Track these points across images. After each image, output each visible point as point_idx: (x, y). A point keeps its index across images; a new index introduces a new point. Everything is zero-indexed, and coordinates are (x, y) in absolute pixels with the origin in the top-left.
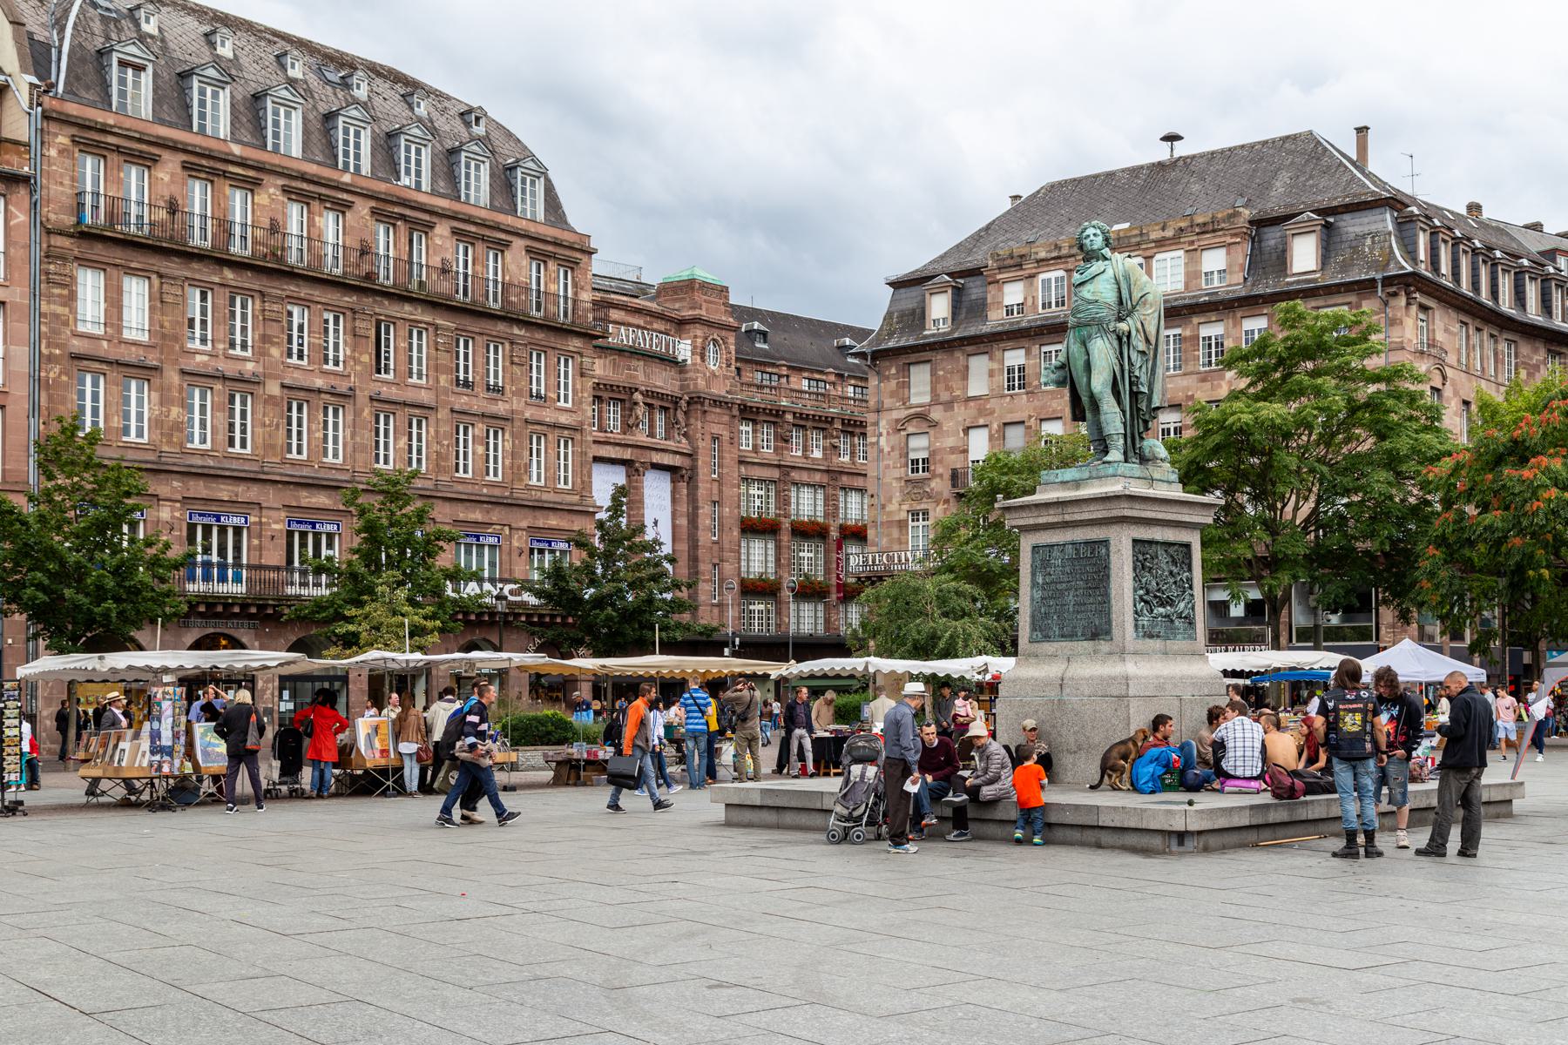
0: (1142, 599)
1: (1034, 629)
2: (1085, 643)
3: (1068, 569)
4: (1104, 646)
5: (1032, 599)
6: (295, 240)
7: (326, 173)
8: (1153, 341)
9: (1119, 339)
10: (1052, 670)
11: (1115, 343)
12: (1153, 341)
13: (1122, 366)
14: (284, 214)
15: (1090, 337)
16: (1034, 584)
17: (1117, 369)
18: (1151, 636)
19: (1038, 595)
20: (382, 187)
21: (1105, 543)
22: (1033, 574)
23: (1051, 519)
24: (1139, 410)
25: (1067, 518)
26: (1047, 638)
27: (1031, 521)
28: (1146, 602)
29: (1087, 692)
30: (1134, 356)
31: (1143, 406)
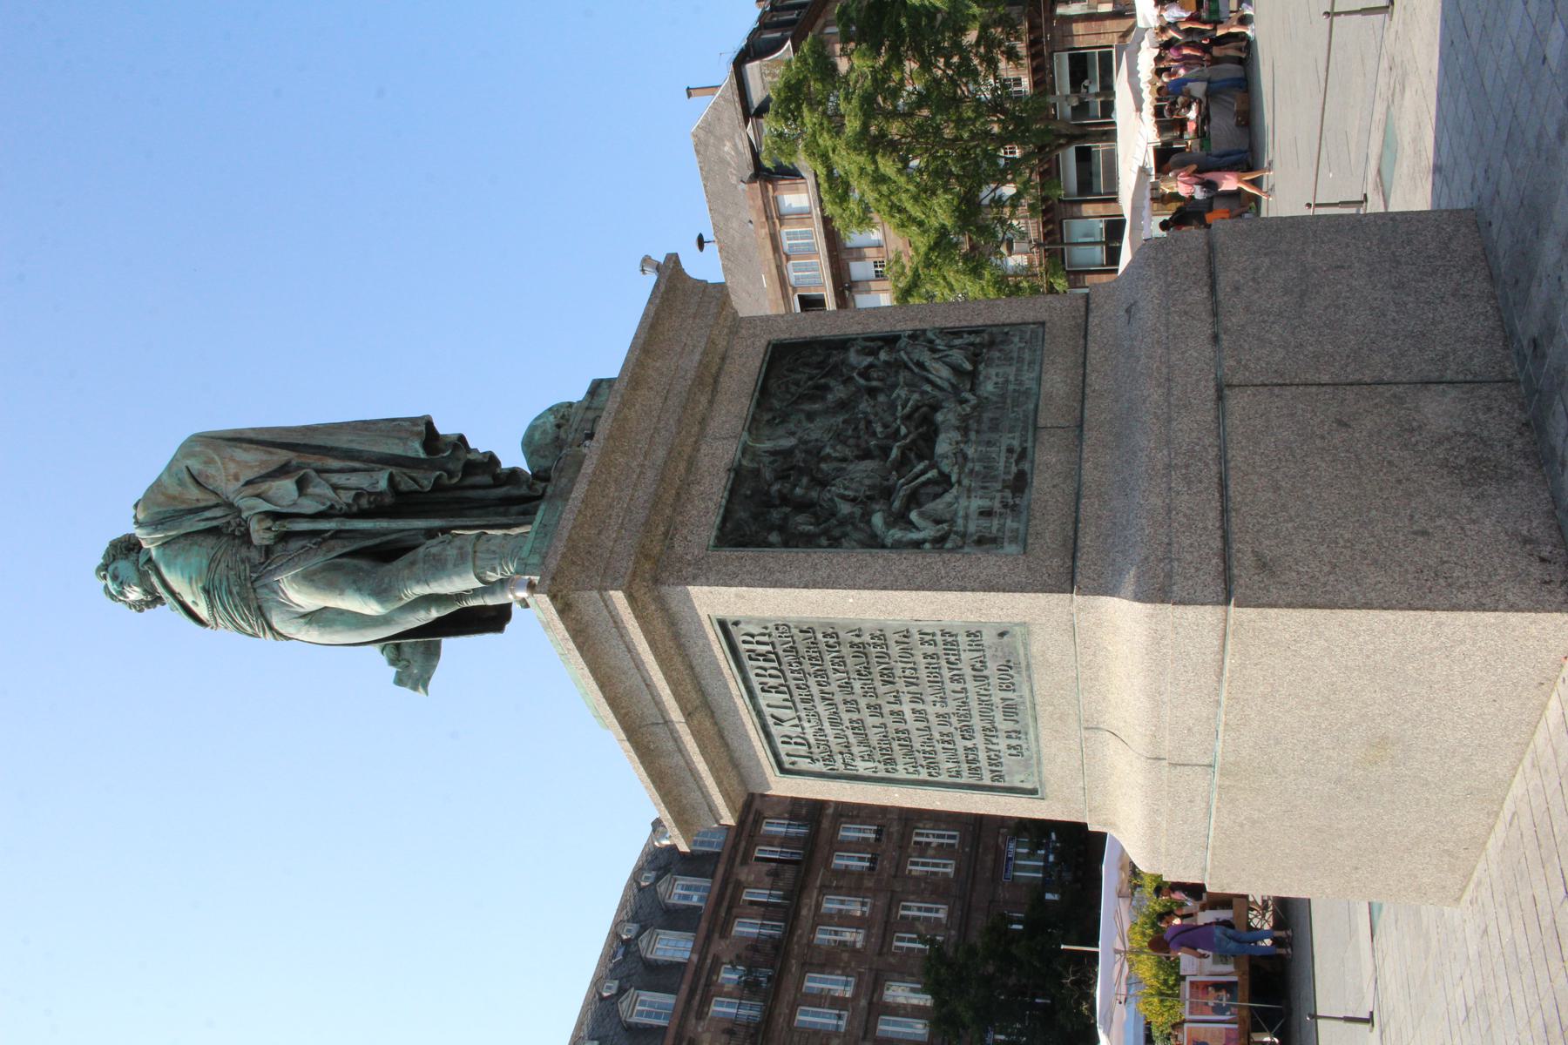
0: (900, 519)
6: (742, 1012)
7: (688, 976)
8: (283, 456)
9: (285, 537)
11: (294, 545)
12: (283, 456)
13: (337, 534)
14: (721, 1020)
17: (340, 547)
18: (1020, 483)
20: (704, 925)
24: (438, 486)
28: (914, 500)
30: (309, 506)
31: (427, 480)
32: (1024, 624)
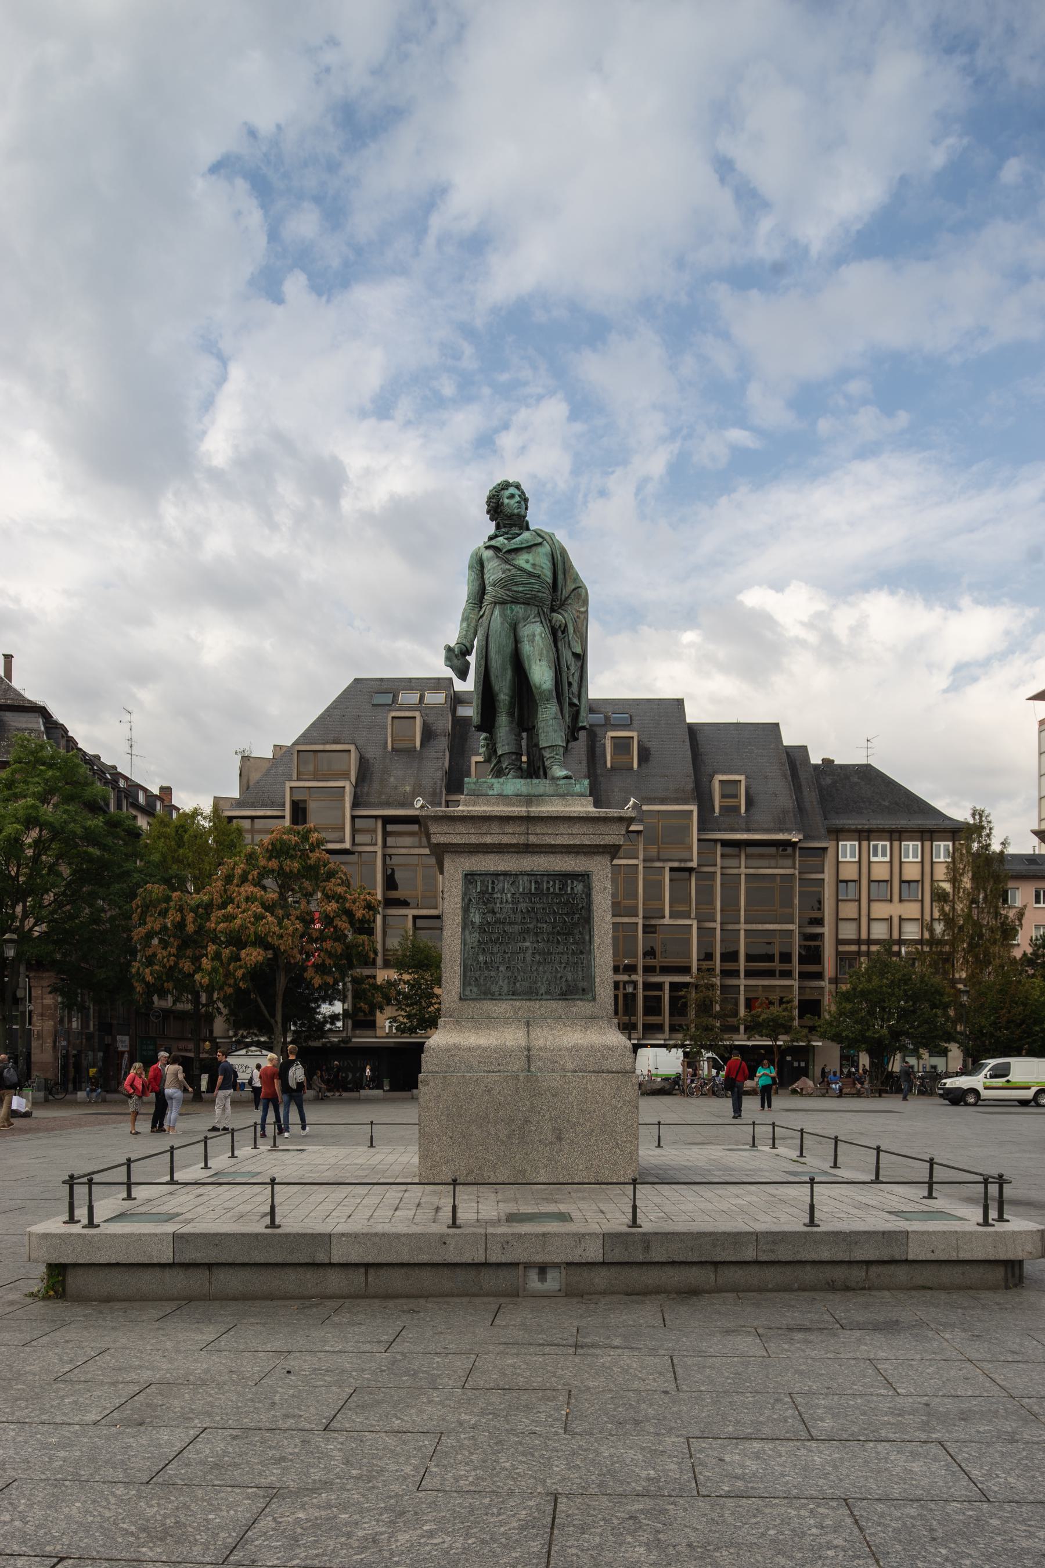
1: (465, 983)
2: (554, 1004)
3: (522, 906)
4: (582, 1007)
5: (464, 943)
10: (512, 1037)
15: (525, 619)
16: (466, 924)
19: (473, 938)
21: (584, 877)
22: (466, 910)
23: (506, 840)
25: (533, 839)
26: (488, 994)
27: (474, 840)
29: (569, 1066)
32: (594, 999)
